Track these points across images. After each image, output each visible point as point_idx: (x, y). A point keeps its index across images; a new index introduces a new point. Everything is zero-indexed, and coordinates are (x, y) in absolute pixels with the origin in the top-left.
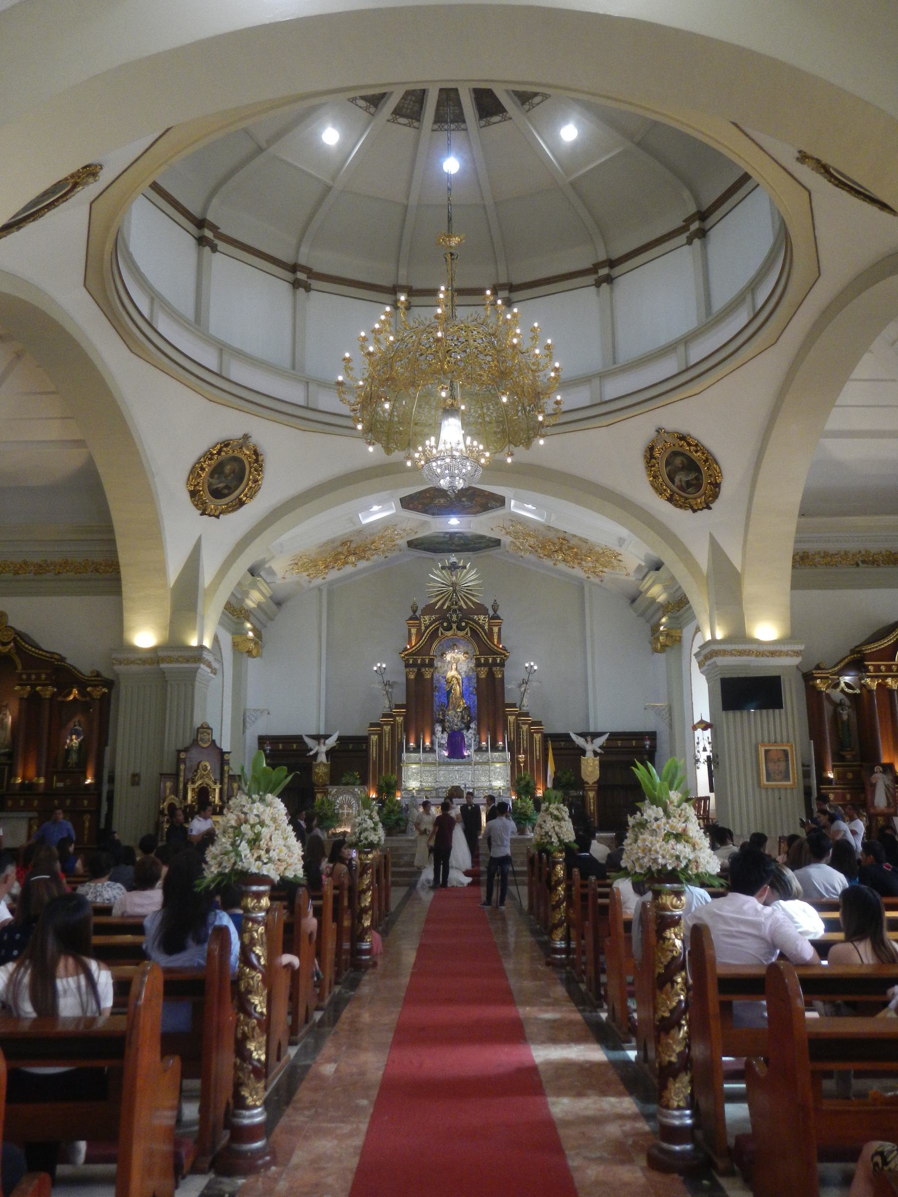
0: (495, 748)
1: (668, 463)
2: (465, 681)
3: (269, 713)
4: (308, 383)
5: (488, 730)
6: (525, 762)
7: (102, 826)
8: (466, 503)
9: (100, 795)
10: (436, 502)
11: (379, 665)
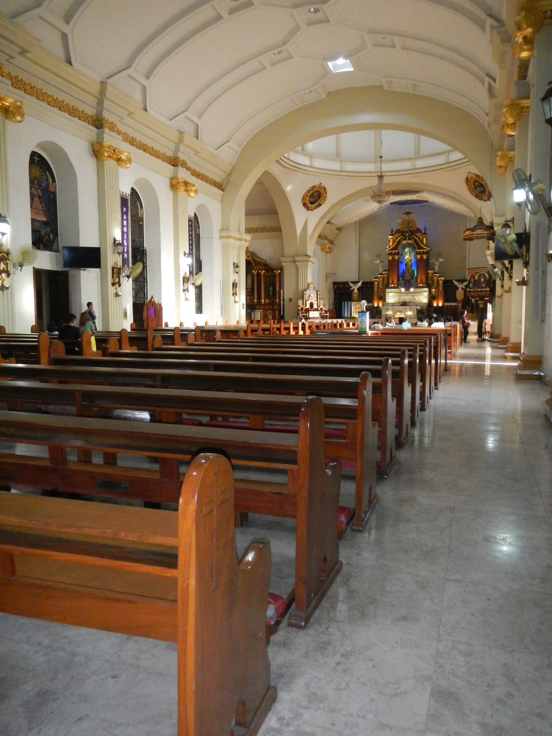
1: (474, 184)
3: (335, 275)
6: (435, 292)
7: (282, 314)
9: (280, 305)
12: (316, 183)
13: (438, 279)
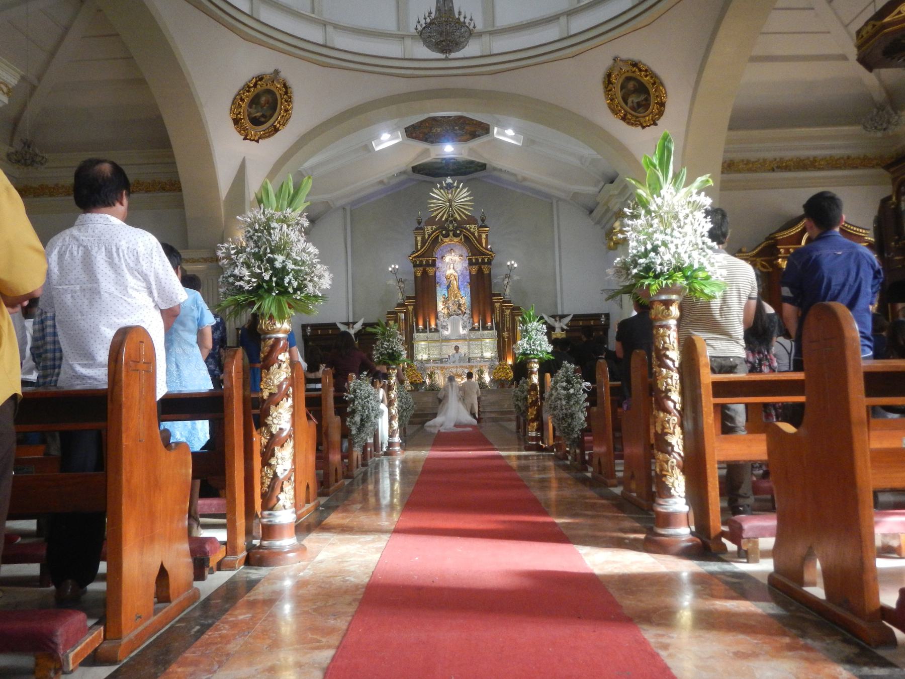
0: (485, 328)
1: (622, 87)
2: (461, 278)
4: (325, 25)
5: (479, 314)
6: (508, 338)
8: (458, 132)
10: (434, 131)
12: (267, 69)
13: (512, 313)
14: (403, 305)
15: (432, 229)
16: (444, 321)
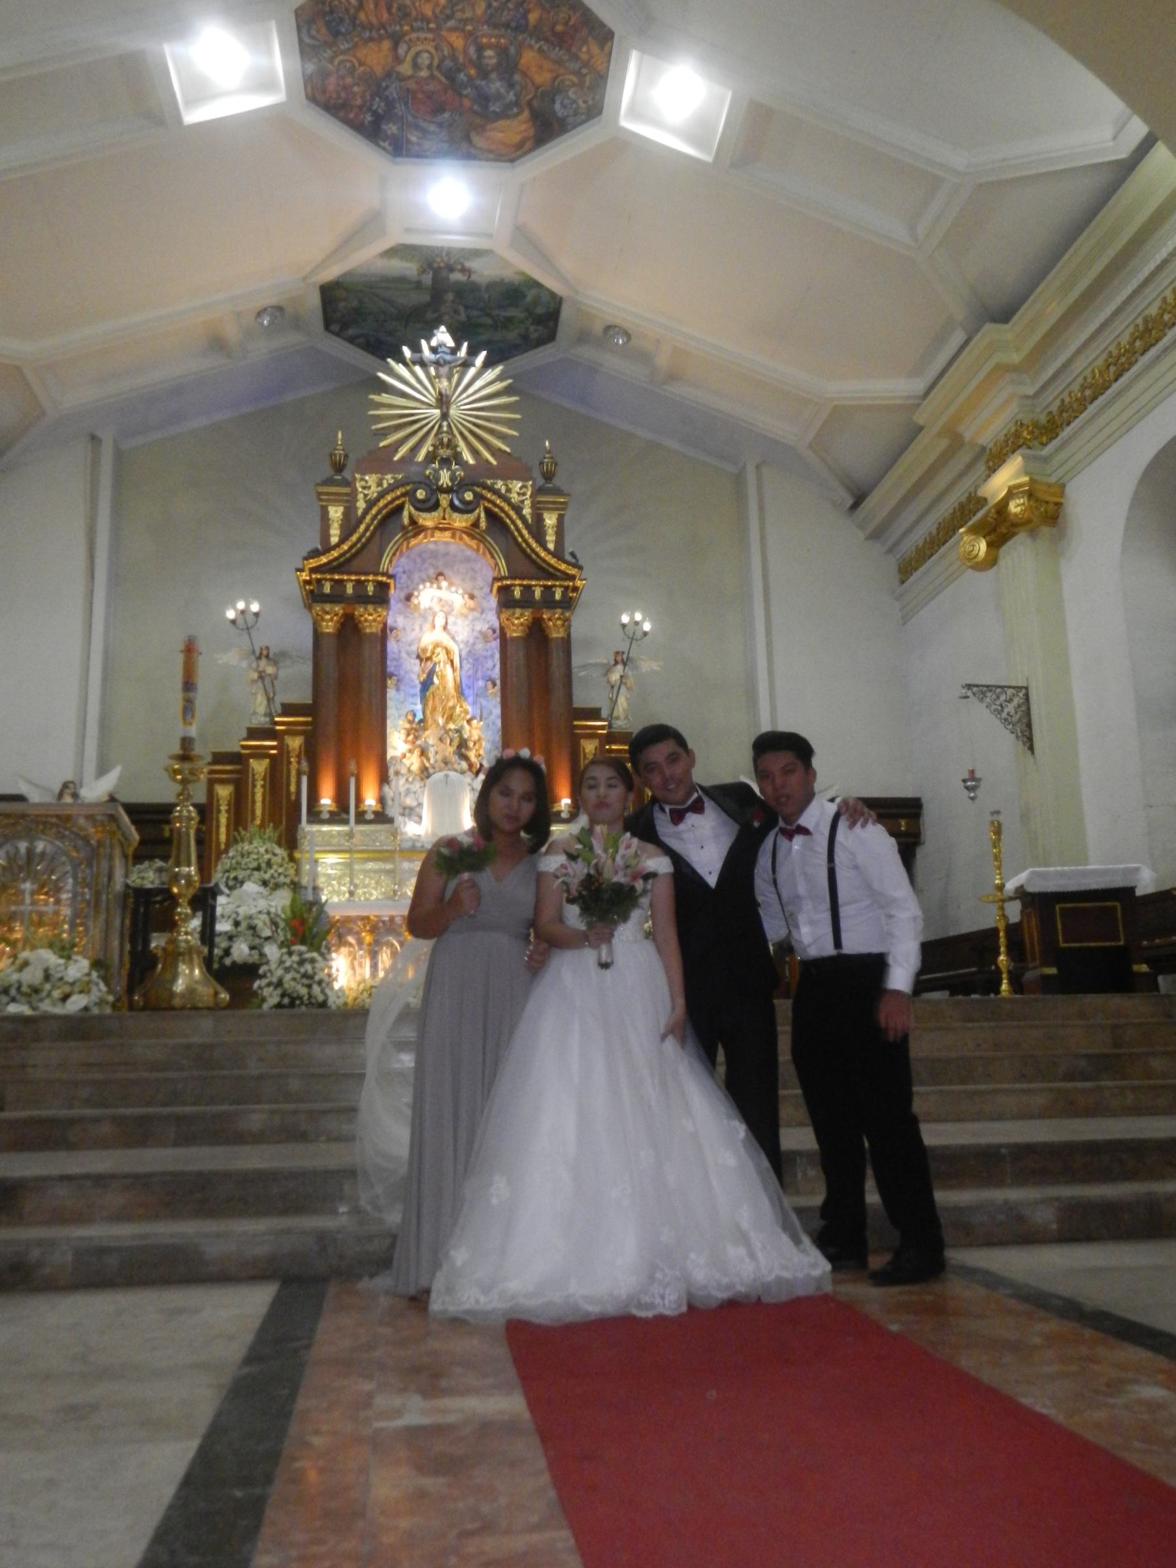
2: (467, 666)
8: (496, 85)
11: (241, 605)
14: (269, 733)
15: (380, 484)
16: (408, 792)
